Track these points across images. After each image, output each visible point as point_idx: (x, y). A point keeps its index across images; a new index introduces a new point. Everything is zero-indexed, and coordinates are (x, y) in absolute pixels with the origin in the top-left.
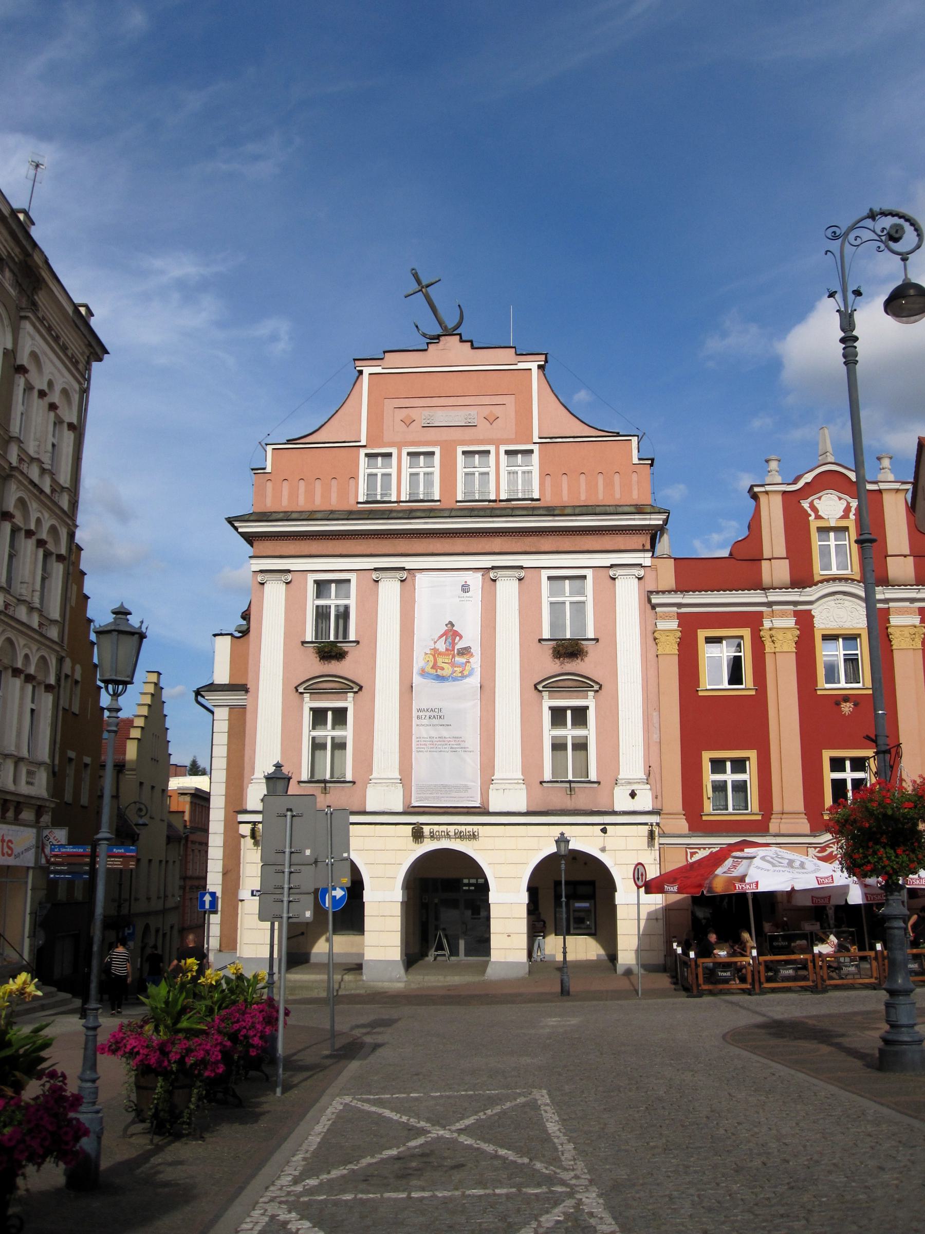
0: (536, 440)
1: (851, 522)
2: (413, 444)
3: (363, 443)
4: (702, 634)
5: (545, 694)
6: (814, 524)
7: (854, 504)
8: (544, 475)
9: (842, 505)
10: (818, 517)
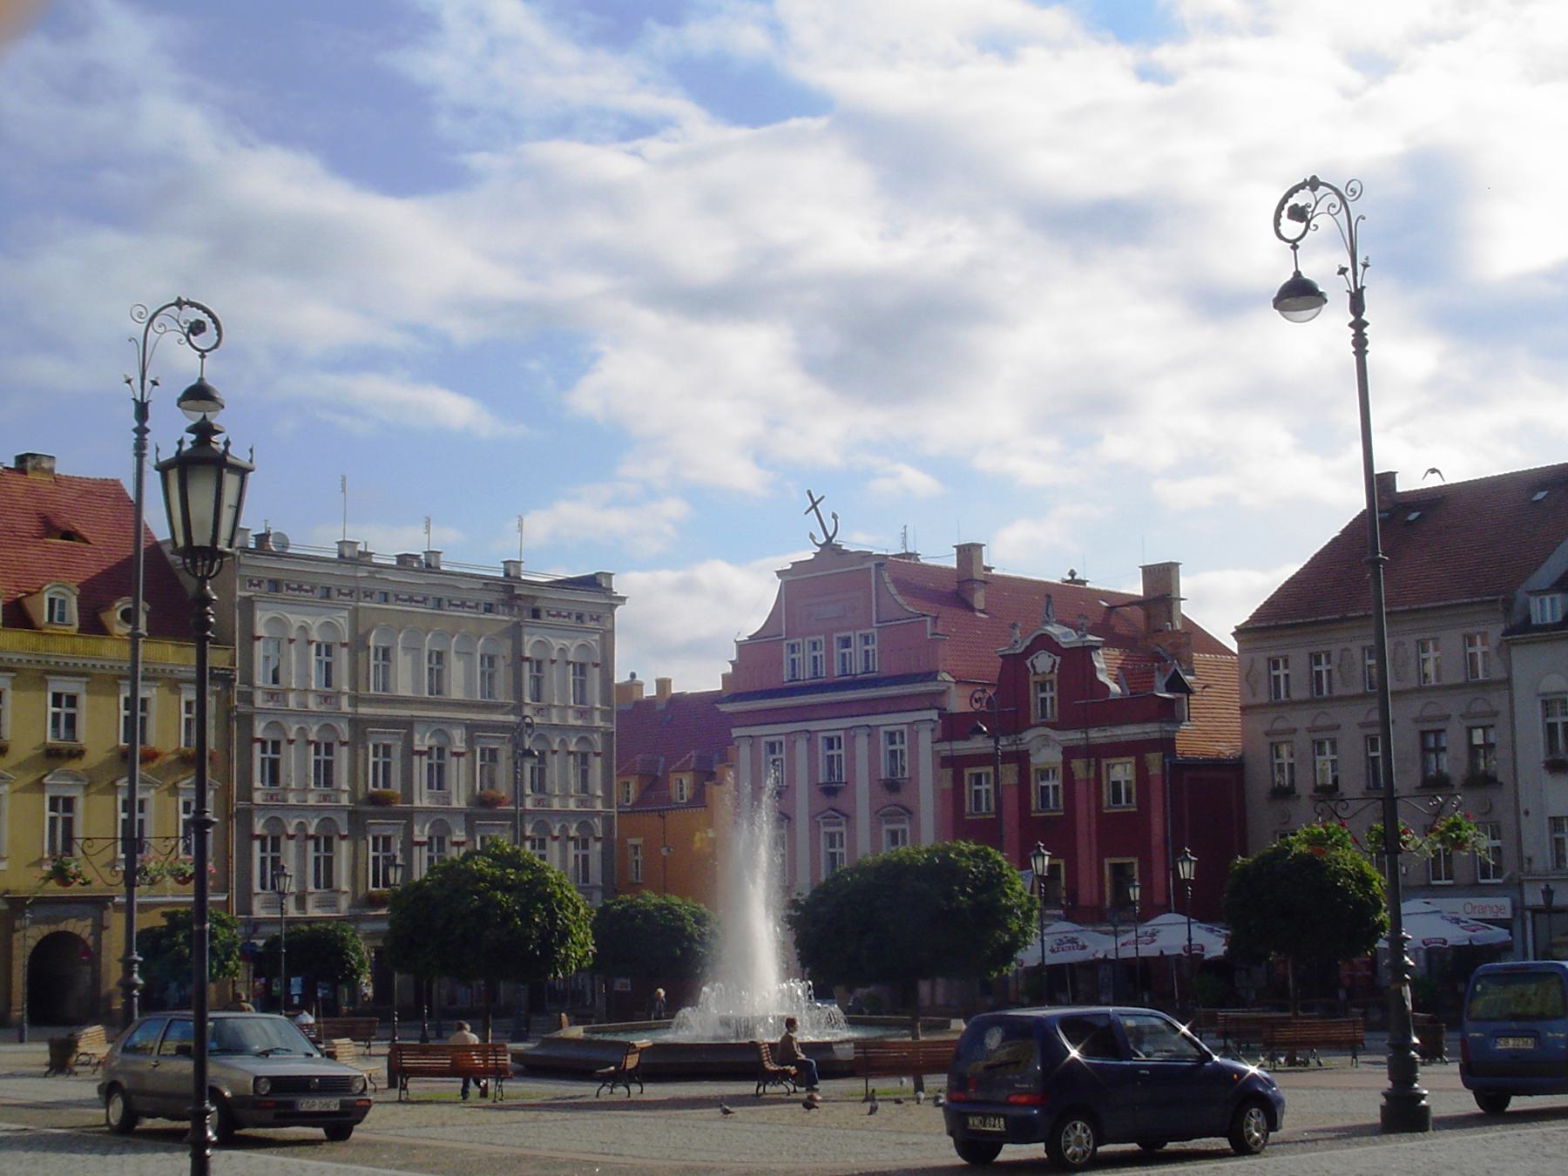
0: (875, 625)
1: (1054, 677)
2: (811, 634)
3: (784, 637)
4: (967, 772)
5: (883, 822)
6: (1032, 679)
7: (1058, 659)
8: (881, 652)
9: (1051, 660)
10: (1036, 673)
